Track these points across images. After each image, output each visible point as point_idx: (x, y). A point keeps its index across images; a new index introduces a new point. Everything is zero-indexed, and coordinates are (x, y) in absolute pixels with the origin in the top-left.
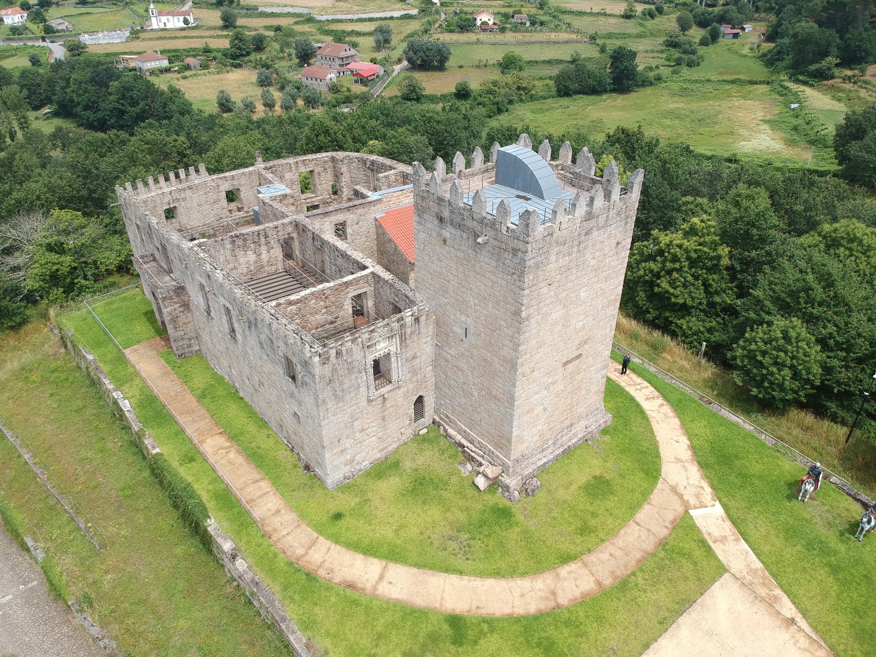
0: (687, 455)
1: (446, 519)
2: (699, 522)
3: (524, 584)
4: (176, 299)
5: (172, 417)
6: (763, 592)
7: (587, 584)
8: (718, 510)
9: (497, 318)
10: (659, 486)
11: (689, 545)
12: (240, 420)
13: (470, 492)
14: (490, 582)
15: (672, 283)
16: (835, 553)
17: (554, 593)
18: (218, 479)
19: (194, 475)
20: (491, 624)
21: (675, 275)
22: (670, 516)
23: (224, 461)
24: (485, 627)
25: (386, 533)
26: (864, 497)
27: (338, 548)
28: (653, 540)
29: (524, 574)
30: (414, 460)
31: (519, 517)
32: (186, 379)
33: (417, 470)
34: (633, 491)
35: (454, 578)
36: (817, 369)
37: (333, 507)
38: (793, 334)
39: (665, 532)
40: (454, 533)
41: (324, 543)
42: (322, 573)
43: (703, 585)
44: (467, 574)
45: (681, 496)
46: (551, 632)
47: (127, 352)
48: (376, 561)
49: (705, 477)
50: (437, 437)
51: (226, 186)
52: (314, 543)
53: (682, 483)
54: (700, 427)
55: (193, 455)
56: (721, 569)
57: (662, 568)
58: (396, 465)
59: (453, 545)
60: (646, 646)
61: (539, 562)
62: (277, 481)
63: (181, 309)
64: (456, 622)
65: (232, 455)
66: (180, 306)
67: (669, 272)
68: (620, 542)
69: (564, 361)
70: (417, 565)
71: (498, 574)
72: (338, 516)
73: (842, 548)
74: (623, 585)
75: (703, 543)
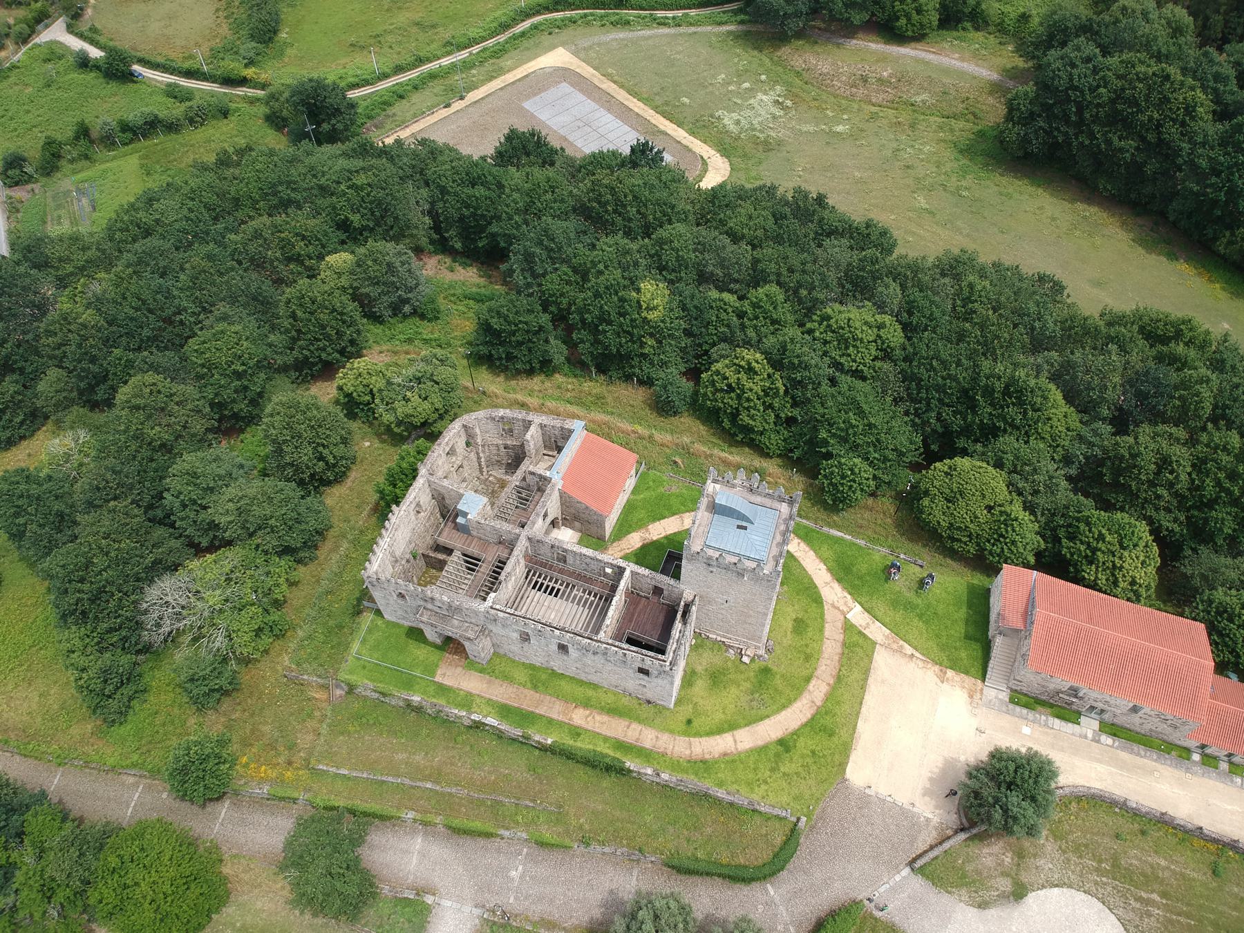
0: (827, 577)
1: (742, 691)
2: (854, 621)
3: (798, 705)
5: (532, 712)
6: (895, 646)
7: (824, 688)
8: (858, 608)
10: (826, 607)
11: (855, 638)
12: (579, 691)
13: (742, 667)
14: (784, 713)
15: (752, 417)
16: (918, 605)
17: (813, 702)
18: (606, 739)
19: (590, 743)
20: (796, 733)
21: (753, 412)
22: (839, 625)
23: (597, 724)
24: (795, 737)
25: (719, 716)
26: (920, 562)
27: (704, 739)
28: (839, 644)
29: (795, 699)
30: (700, 664)
31: (775, 669)
32: (507, 678)
33: (706, 670)
34: (816, 619)
35: (767, 721)
36: (872, 483)
37: (682, 718)
38: (857, 470)
39: (842, 636)
40: (751, 697)
41: (695, 741)
42: (707, 756)
43: (870, 657)
44: (772, 715)
45: (838, 608)
46: (822, 721)
47: (438, 679)
48: (726, 735)
49: (844, 588)
50: (702, 641)
51: (413, 506)
52: (690, 744)
53: (836, 599)
54: (827, 553)
55: (576, 732)
56: (874, 643)
57: (849, 659)
58: (693, 672)
59: (755, 703)
60: (861, 703)
61: (798, 689)
62: (639, 720)
64: (781, 742)
65: (598, 718)
67: (748, 409)
68: (826, 655)
70: (746, 725)
71: (784, 707)
72: (689, 722)
73: (919, 601)
74: (839, 679)
75: (860, 632)
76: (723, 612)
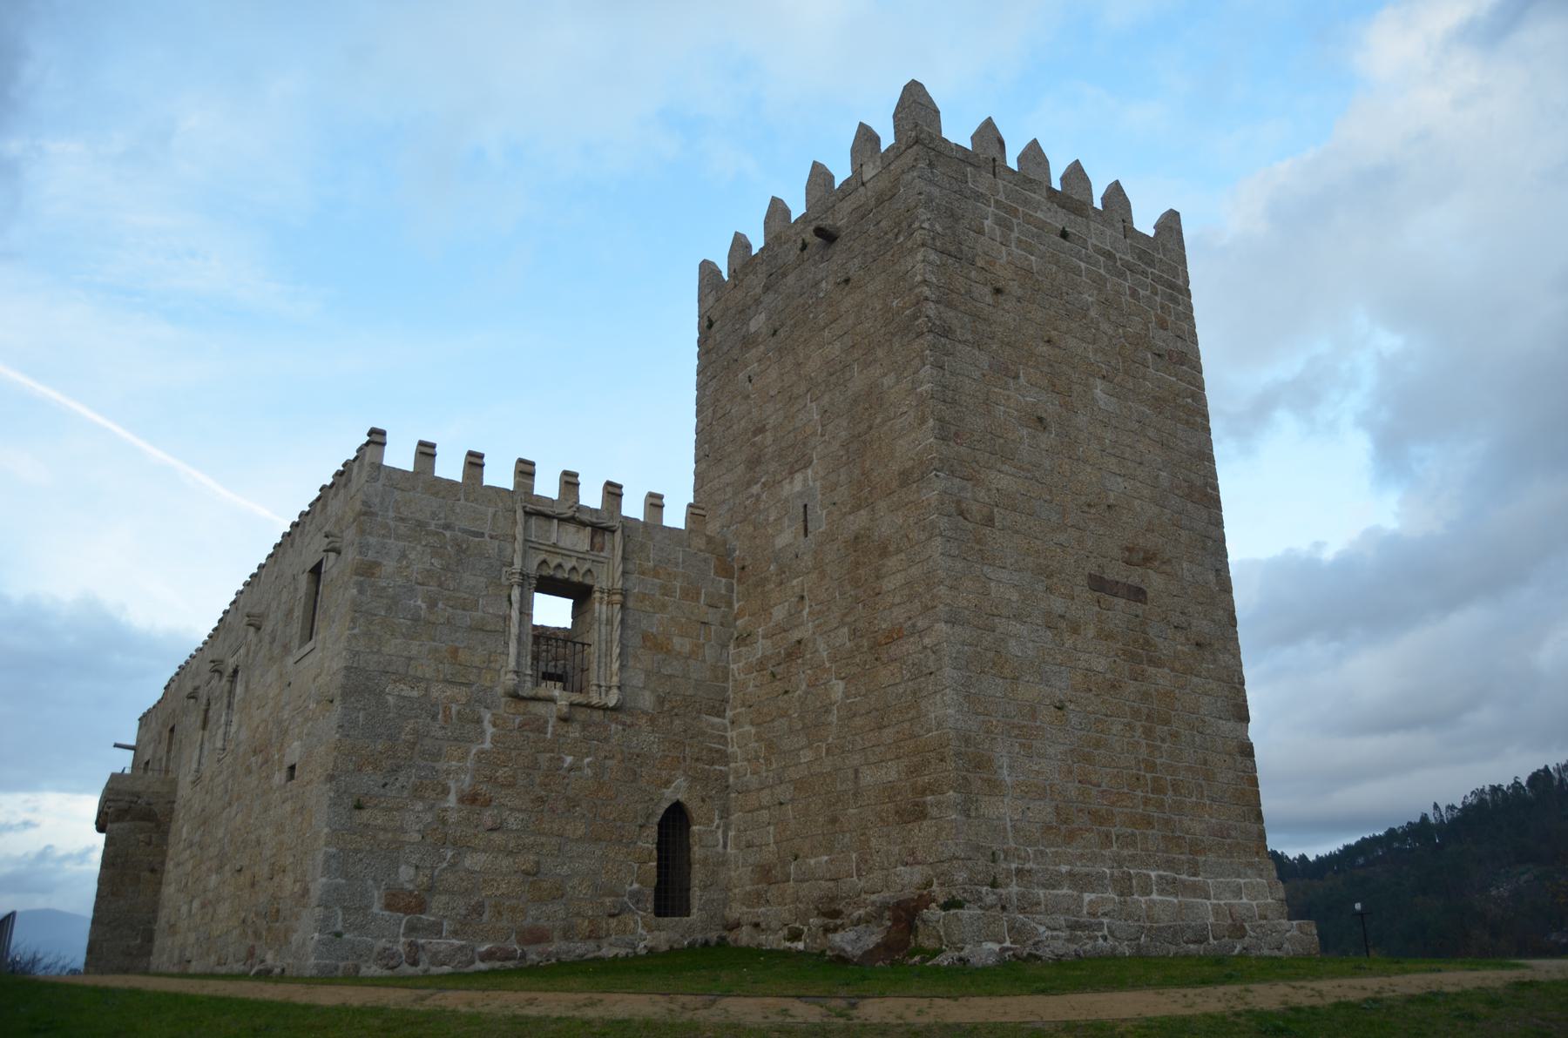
69: (1091, 567)
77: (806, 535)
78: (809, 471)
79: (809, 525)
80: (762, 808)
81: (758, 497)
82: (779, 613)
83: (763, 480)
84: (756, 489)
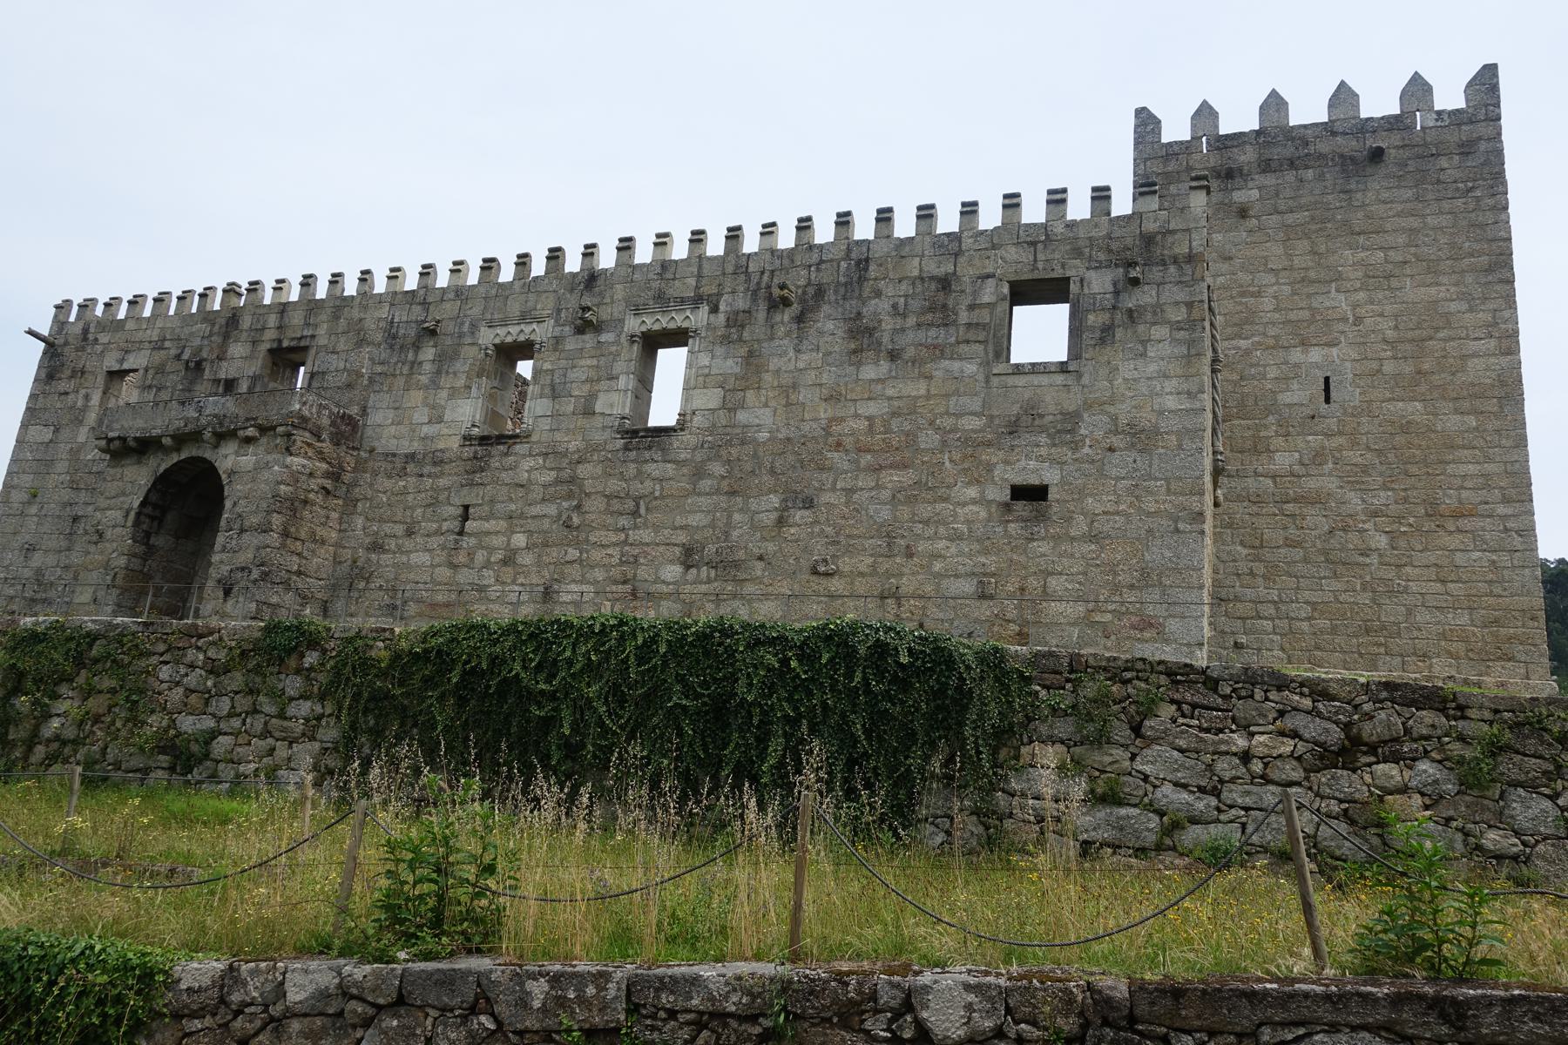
4: (326, 446)
9: (1436, 302)
63: (328, 484)
66: (327, 475)
76: (1325, 481)
77: (1327, 400)
78: (1334, 351)
79: (1333, 394)
80: (1261, 618)
81: (1248, 352)
82: (1283, 460)
83: (1256, 339)
84: (1243, 343)
